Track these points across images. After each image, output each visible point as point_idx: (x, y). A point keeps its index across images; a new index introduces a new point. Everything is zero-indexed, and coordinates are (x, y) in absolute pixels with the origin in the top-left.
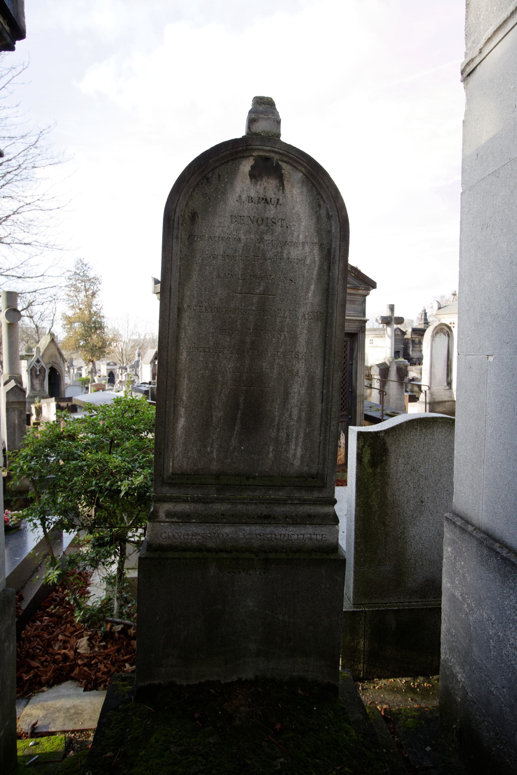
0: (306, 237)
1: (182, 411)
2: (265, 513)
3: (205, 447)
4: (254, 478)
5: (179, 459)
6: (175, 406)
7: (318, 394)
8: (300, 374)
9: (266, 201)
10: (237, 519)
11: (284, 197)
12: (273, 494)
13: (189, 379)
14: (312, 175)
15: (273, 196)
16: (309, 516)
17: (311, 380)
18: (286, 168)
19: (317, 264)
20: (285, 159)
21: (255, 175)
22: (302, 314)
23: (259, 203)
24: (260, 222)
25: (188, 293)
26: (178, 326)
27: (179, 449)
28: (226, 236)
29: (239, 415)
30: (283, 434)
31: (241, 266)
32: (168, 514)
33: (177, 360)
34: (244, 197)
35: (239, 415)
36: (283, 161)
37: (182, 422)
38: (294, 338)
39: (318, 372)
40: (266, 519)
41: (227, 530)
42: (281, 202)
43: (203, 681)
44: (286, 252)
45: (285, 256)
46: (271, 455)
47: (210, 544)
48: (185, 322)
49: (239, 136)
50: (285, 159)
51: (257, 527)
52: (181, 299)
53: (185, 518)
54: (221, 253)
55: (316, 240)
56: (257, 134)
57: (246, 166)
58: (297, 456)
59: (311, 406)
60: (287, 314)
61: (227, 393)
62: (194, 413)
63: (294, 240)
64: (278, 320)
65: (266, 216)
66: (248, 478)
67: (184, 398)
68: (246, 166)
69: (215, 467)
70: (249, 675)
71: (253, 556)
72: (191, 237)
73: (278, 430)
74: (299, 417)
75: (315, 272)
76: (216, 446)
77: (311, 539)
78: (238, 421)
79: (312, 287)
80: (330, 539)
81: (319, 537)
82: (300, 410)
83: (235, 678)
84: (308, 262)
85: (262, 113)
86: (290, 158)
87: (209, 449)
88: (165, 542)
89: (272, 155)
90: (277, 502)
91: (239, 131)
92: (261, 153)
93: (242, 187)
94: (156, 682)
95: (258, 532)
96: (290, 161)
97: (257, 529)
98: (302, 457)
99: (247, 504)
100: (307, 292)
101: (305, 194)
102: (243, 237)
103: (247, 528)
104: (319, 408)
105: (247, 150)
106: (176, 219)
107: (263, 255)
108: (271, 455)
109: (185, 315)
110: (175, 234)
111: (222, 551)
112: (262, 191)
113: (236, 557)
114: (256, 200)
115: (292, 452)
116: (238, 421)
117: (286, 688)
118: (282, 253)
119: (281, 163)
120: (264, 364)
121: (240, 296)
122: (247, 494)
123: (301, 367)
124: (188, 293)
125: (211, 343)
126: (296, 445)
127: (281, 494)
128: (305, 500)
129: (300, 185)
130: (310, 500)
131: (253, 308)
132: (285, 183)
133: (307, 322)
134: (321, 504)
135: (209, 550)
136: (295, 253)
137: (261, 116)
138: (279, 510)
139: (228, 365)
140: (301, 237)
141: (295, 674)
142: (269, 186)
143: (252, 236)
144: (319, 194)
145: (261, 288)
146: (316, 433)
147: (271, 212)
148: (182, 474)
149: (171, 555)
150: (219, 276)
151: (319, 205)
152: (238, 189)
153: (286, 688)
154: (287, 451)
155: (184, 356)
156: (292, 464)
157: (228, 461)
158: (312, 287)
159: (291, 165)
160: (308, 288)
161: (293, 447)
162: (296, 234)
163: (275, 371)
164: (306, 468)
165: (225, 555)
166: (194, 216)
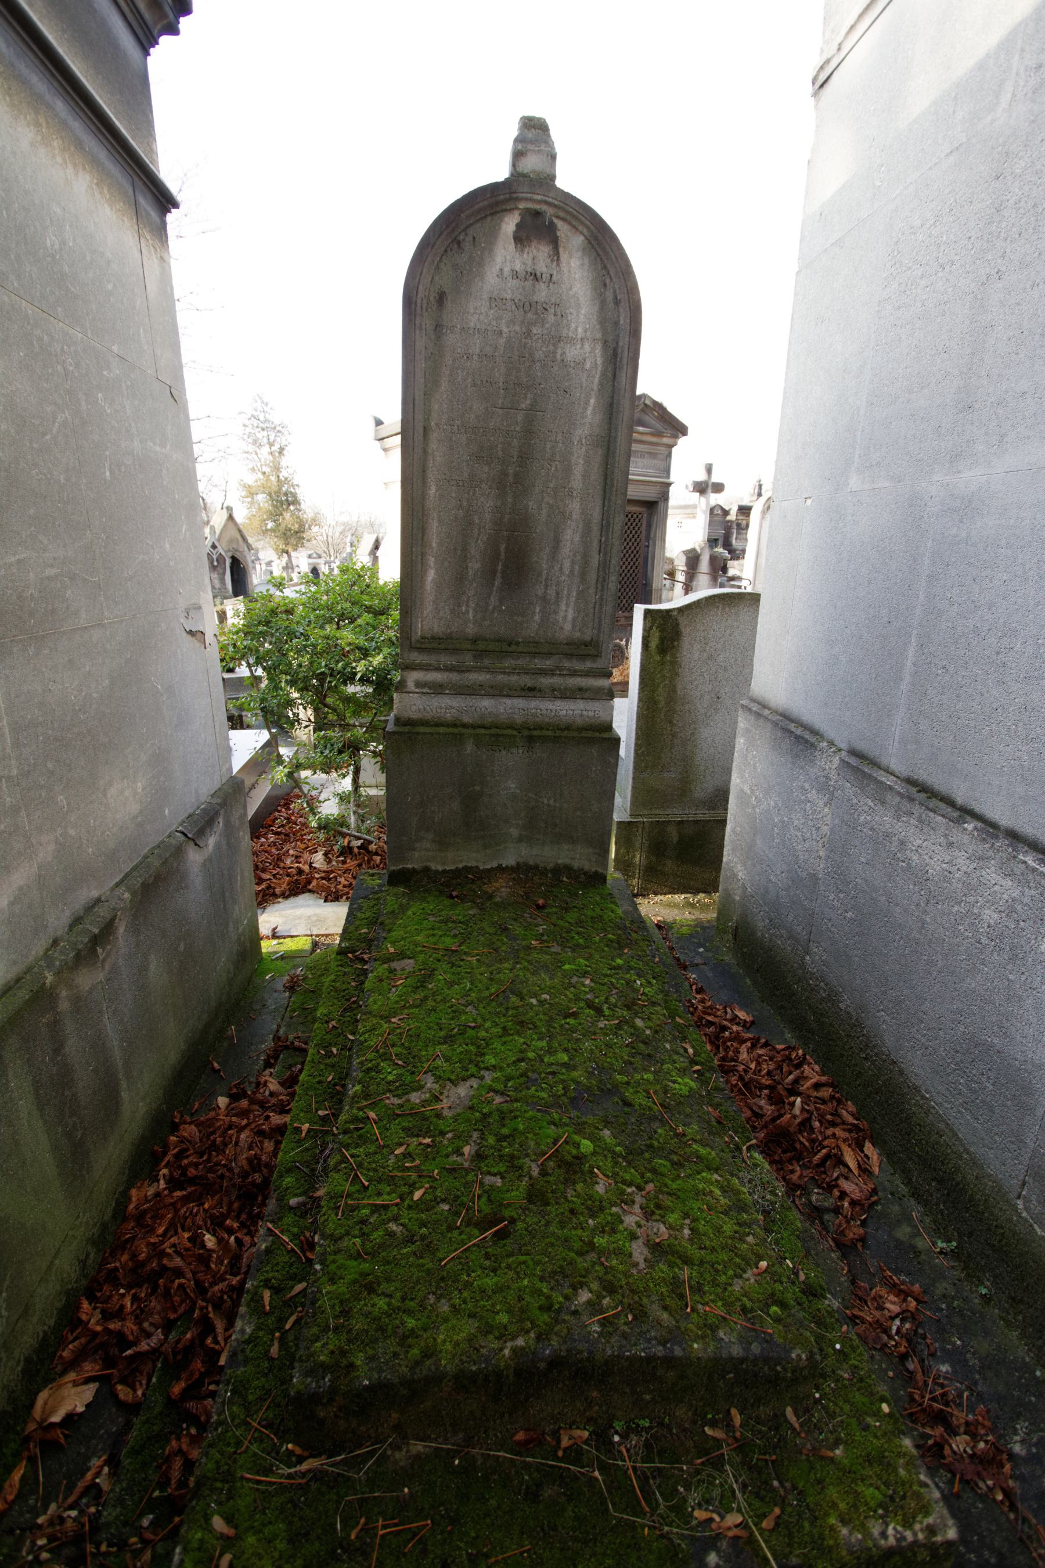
0: (585, 332)
1: (431, 561)
2: (529, 685)
3: (459, 606)
4: (518, 644)
5: (430, 620)
6: (423, 555)
7: (595, 544)
8: (574, 517)
9: (535, 277)
10: (498, 692)
11: (559, 272)
12: (538, 663)
13: (439, 521)
14: (596, 238)
15: (544, 270)
16: (581, 689)
17: (587, 525)
18: (563, 229)
19: (600, 368)
20: (562, 214)
21: (521, 239)
22: (578, 438)
23: (526, 279)
24: (527, 308)
25: (436, 407)
26: (425, 451)
27: (428, 609)
28: (483, 327)
29: (500, 567)
30: (552, 592)
31: (503, 370)
32: (418, 684)
33: (424, 496)
34: (507, 270)
35: (500, 567)
36: (558, 217)
37: (431, 575)
38: (568, 470)
39: (596, 515)
40: (531, 692)
41: (486, 704)
42: (554, 278)
43: (460, 866)
44: (559, 351)
45: (558, 357)
46: (537, 617)
47: (466, 719)
48: (433, 446)
49: (501, 179)
50: (562, 214)
51: (520, 700)
52: (428, 414)
53: (437, 689)
54: (477, 351)
55: (599, 336)
56: (525, 176)
57: (509, 224)
58: (567, 619)
59: (586, 557)
60: (559, 437)
61: (485, 538)
62: (446, 564)
63: (571, 334)
64: (549, 445)
65: (535, 298)
66: (510, 644)
67: (434, 545)
68: (509, 224)
69: (471, 630)
70: (510, 861)
71: (515, 733)
72: (438, 327)
73: (546, 586)
74: (572, 571)
75: (596, 381)
76: (472, 605)
77: (582, 715)
78: (499, 575)
79: (592, 401)
80: (603, 716)
81: (591, 714)
82: (573, 562)
83: (495, 865)
84: (588, 366)
85: (531, 142)
86: (568, 212)
87: (464, 608)
88: (415, 716)
89: (544, 208)
90: (543, 672)
91: (499, 171)
92: (530, 205)
93: (505, 257)
94: (410, 866)
95: (521, 706)
96: (569, 218)
97: (520, 703)
98: (574, 620)
99: (508, 674)
100: (585, 408)
101: (586, 267)
102: (505, 330)
103: (509, 702)
104: (595, 560)
105: (511, 199)
106: (419, 301)
107: (531, 355)
108: (537, 617)
109: (434, 436)
110: (417, 322)
111: (479, 727)
112: (530, 263)
113: (497, 734)
114: (522, 275)
115: (562, 614)
116: (499, 575)
117: (550, 875)
118: (555, 352)
119: (555, 221)
120: (530, 503)
121: (500, 411)
122: (509, 662)
123: (575, 507)
124: (436, 407)
125: (466, 475)
126: (567, 605)
127: (549, 663)
128: (576, 671)
129: (580, 254)
130: (582, 671)
131: (518, 429)
132: (561, 250)
133: (583, 449)
134: (594, 676)
135: (464, 726)
136: (572, 353)
137: (530, 147)
138: (546, 681)
139: (487, 503)
140: (580, 330)
141: (560, 861)
142: (539, 254)
143: (517, 328)
144: (605, 267)
145: (528, 402)
146: (592, 591)
147: (542, 293)
148: (433, 638)
149: (422, 729)
150: (474, 385)
151: (605, 285)
152: (499, 259)
153: (550, 875)
154: (556, 613)
155: (432, 491)
156: (562, 628)
157: (487, 623)
158: (592, 401)
159: (570, 224)
160: (587, 403)
161: (563, 608)
162: (573, 326)
163: (544, 512)
164: (578, 634)
165: (483, 731)
166: (441, 298)
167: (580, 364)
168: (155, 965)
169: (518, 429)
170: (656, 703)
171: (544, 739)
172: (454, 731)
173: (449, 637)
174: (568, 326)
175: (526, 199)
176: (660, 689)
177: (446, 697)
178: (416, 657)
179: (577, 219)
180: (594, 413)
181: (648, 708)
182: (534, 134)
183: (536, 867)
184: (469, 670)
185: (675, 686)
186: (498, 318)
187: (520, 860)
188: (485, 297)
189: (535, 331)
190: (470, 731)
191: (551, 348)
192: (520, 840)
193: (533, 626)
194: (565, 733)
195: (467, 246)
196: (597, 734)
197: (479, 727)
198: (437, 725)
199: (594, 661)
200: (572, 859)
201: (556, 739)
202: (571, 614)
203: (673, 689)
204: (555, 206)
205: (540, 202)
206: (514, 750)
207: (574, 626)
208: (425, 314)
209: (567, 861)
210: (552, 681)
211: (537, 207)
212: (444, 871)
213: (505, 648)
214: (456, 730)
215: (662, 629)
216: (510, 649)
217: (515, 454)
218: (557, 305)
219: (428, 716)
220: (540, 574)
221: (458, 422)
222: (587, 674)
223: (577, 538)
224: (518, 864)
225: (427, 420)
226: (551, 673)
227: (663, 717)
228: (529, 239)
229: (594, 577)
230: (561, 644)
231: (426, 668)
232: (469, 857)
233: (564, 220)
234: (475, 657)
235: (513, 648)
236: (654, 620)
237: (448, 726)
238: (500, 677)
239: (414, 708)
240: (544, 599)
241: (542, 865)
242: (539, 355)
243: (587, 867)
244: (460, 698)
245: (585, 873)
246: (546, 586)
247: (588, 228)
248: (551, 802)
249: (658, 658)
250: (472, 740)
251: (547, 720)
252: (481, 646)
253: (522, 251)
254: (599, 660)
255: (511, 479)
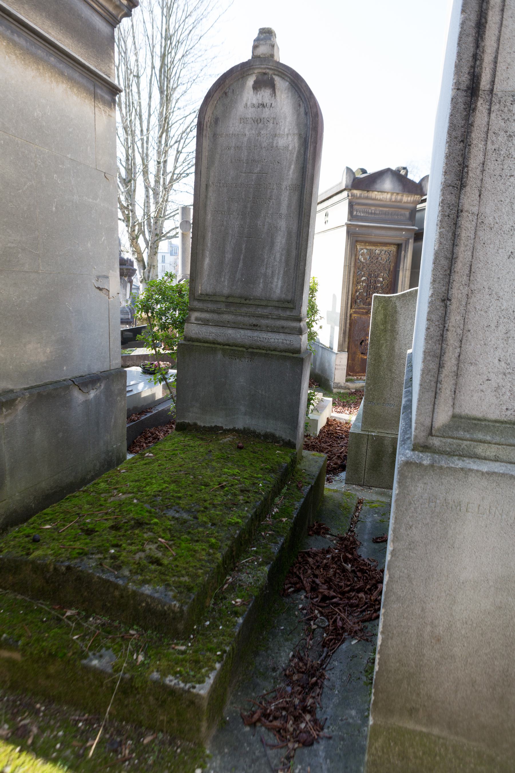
0: (289, 130)
1: (207, 253)
2: (254, 323)
3: (220, 278)
4: (250, 299)
5: (205, 286)
6: (203, 250)
7: (294, 244)
8: (282, 229)
9: (263, 105)
10: (236, 326)
11: (276, 101)
12: (260, 311)
13: (212, 232)
14: (294, 82)
15: (268, 101)
16: (283, 327)
17: (289, 233)
18: (277, 80)
19: (297, 149)
20: (276, 73)
21: (257, 86)
22: (285, 186)
23: (258, 107)
24: (259, 121)
25: (212, 174)
26: (206, 197)
27: (205, 279)
28: (237, 133)
29: (242, 257)
30: (269, 271)
31: (246, 154)
32: (197, 319)
33: (205, 219)
34: (249, 104)
35: (242, 257)
36: (275, 74)
37: (207, 261)
38: (279, 204)
39: (295, 228)
40: (254, 327)
41: (230, 331)
42: (273, 105)
43: (213, 425)
44: (275, 142)
45: (275, 145)
46: (261, 285)
47: (220, 340)
48: (210, 194)
49: (245, 60)
50: (276, 73)
51: (249, 331)
52: (208, 178)
53: (206, 323)
54: (234, 145)
55: (296, 132)
56: (259, 57)
57: (250, 82)
58: (278, 287)
59: (289, 252)
60: (275, 186)
61: (235, 242)
62: (215, 255)
63: (281, 133)
64: (269, 191)
65: (263, 116)
66: (246, 300)
67: (209, 245)
68: (250, 82)
69: (226, 291)
70: (240, 425)
71: (245, 349)
72: (215, 135)
73: (266, 269)
74: (281, 260)
75: (295, 156)
76: (227, 277)
77: (283, 343)
78: (241, 261)
79: (293, 167)
80: (296, 345)
81: (288, 342)
82: (281, 255)
83: (231, 427)
84: (290, 148)
85: (262, 40)
86: (279, 72)
87: (223, 279)
88: (194, 336)
89: (268, 71)
90: (262, 316)
91: (246, 56)
92: (260, 71)
93: (248, 96)
94: (186, 421)
95: (249, 335)
96: (280, 74)
97: (249, 333)
98: (282, 287)
99: (244, 316)
100: (289, 171)
101: (290, 97)
102: (247, 133)
103: (242, 332)
104: (294, 253)
105: (250, 69)
106: (205, 123)
107: (260, 145)
108: (261, 285)
109: (211, 189)
110: (204, 134)
111: (227, 345)
112: (260, 99)
113: (234, 350)
114: (256, 105)
115: (275, 284)
116: (241, 261)
117: (262, 438)
118: (273, 143)
119: (274, 76)
120: (259, 222)
121: (244, 175)
122: (244, 310)
123: (283, 224)
124: (212, 174)
125: (226, 208)
126: (278, 279)
127: (266, 311)
128: (280, 317)
129: (286, 91)
130: (284, 317)
131: (253, 183)
132: (276, 91)
133: (288, 192)
134: (291, 320)
135: (219, 344)
136: (281, 142)
137: (261, 42)
138: (264, 322)
139: (235, 223)
140: (286, 130)
141: (268, 430)
142: (265, 95)
143: (253, 132)
144: (300, 96)
145: (258, 169)
146: (292, 271)
147: (266, 113)
148: (207, 295)
149: (196, 344)
150: (231, 162)
151: (300, 105)
152: (245, 99)
153: (262, 438)
154: (272, 283)
155: (209, 217)
156: (275, 292)
157: (234, 287)
158: (293, 167)
159: (281, 77)
160: (290, 167)
161: (276, 280)
162: (282, 128)
163: (266, 227)
164: (284, 296)
165: (227, 347)
166: (216, 121)
167: (286, 148)
168: (38, 434)
169: (253, 183)
170: (380, 357)
171: (260, 355)
172: (212, 346)
173: (215, 295)
174: (280, 129)
175: (258, 68)
176: (383, 348)
177: (210, 327)
178: (197, 304)
179: (284, 74)
180: (293, 173)
181: (375, 360)
182: (266, 35)
183: (254, 432)
184: (222, 313)
185: (394, 347)
186: (244, 128)
187: (246, 426)
188: (238, 118)
189: (262, 133)
190: (221, 347)
191: (271, 140)
192: (245, 414)
193: (258, 291)
194: (273, 352)
195: (230, 94)
196: (291, 355)
197: (227, 345)
198: (205, 342)
199: (291, 311)
200: (275, 430)
201: (266, 355)
202: (280, 283)
203: (393, 349)
204: (272, 69)
205: (265, 68)
206: (243, 360)
207: (281, 291)
208: (208, 129)
209: (273, 431)
210: (267, 321)
211: (264, 71)
212: (204, 427)
213: (243, 301)
214: (213, 346)
215: (385, 308)
216: (245, 302)
217: (251, 196)
218: (274, 118)
219: (201, 337)
220: (263, 261)
221: (223, 182)
222: (287, 319)
223: (284, 241)
224: (244, 428)
225: (208, 181)
226: (266, 317)
227: (385, 366)
228: (260, 88)
229: (293, 263)
230: (274, 301)
231: (201, 310)
232: (217, 420)
233: (278, 76)
234: (226, 306)
235: (247, 301)
236: (380, 302)
237: (210, 343)
238: (239, 318)
239: (193, 332)
240: (265, 275)
241: (258, 431)
242: (264, 144)
243: (284, 437)
244: (217, 328)
245: (283, 440)
246: (266, 269)
247: (289, 78)
248: (263, 392)
249: (382, 327)
250: (220, 352)
251: (263, 344)
252: (231, 300)
253: (257, 93)
254: (294, 311)
255: (249, 210)
